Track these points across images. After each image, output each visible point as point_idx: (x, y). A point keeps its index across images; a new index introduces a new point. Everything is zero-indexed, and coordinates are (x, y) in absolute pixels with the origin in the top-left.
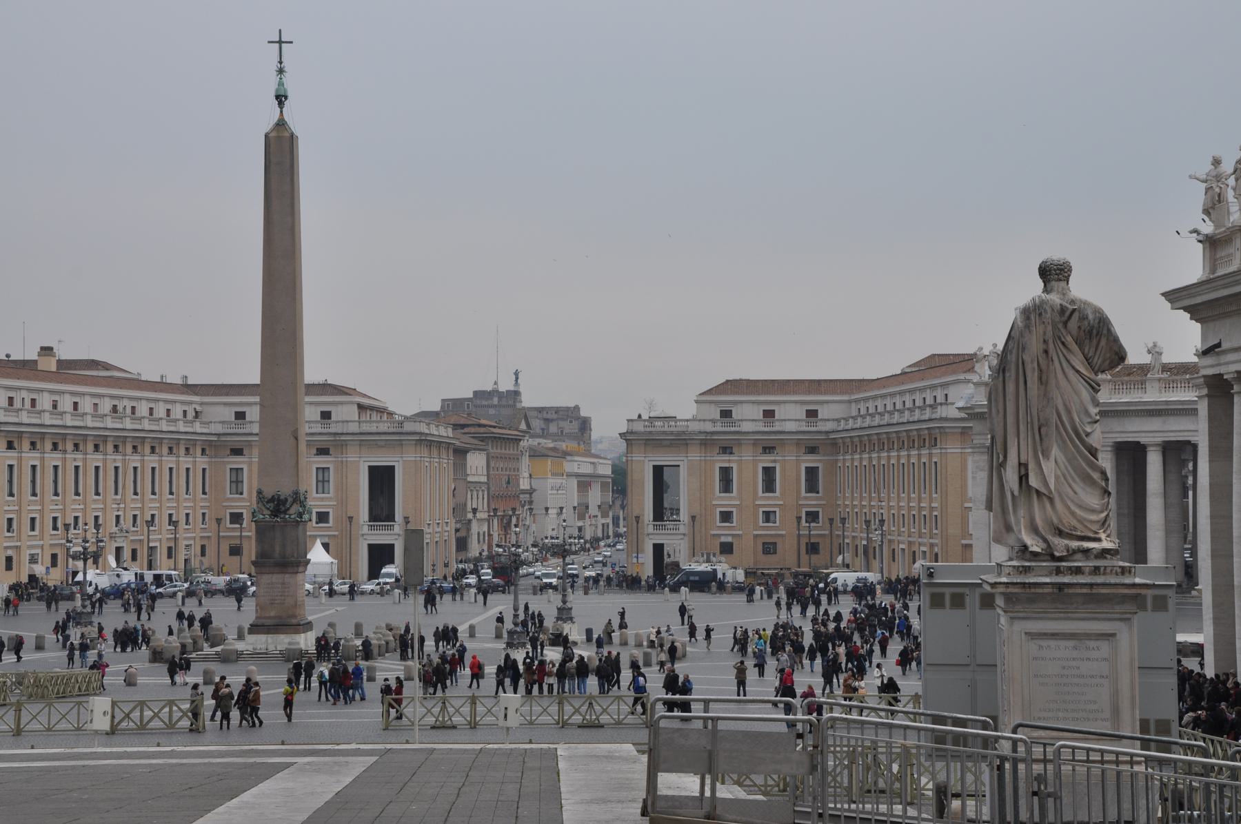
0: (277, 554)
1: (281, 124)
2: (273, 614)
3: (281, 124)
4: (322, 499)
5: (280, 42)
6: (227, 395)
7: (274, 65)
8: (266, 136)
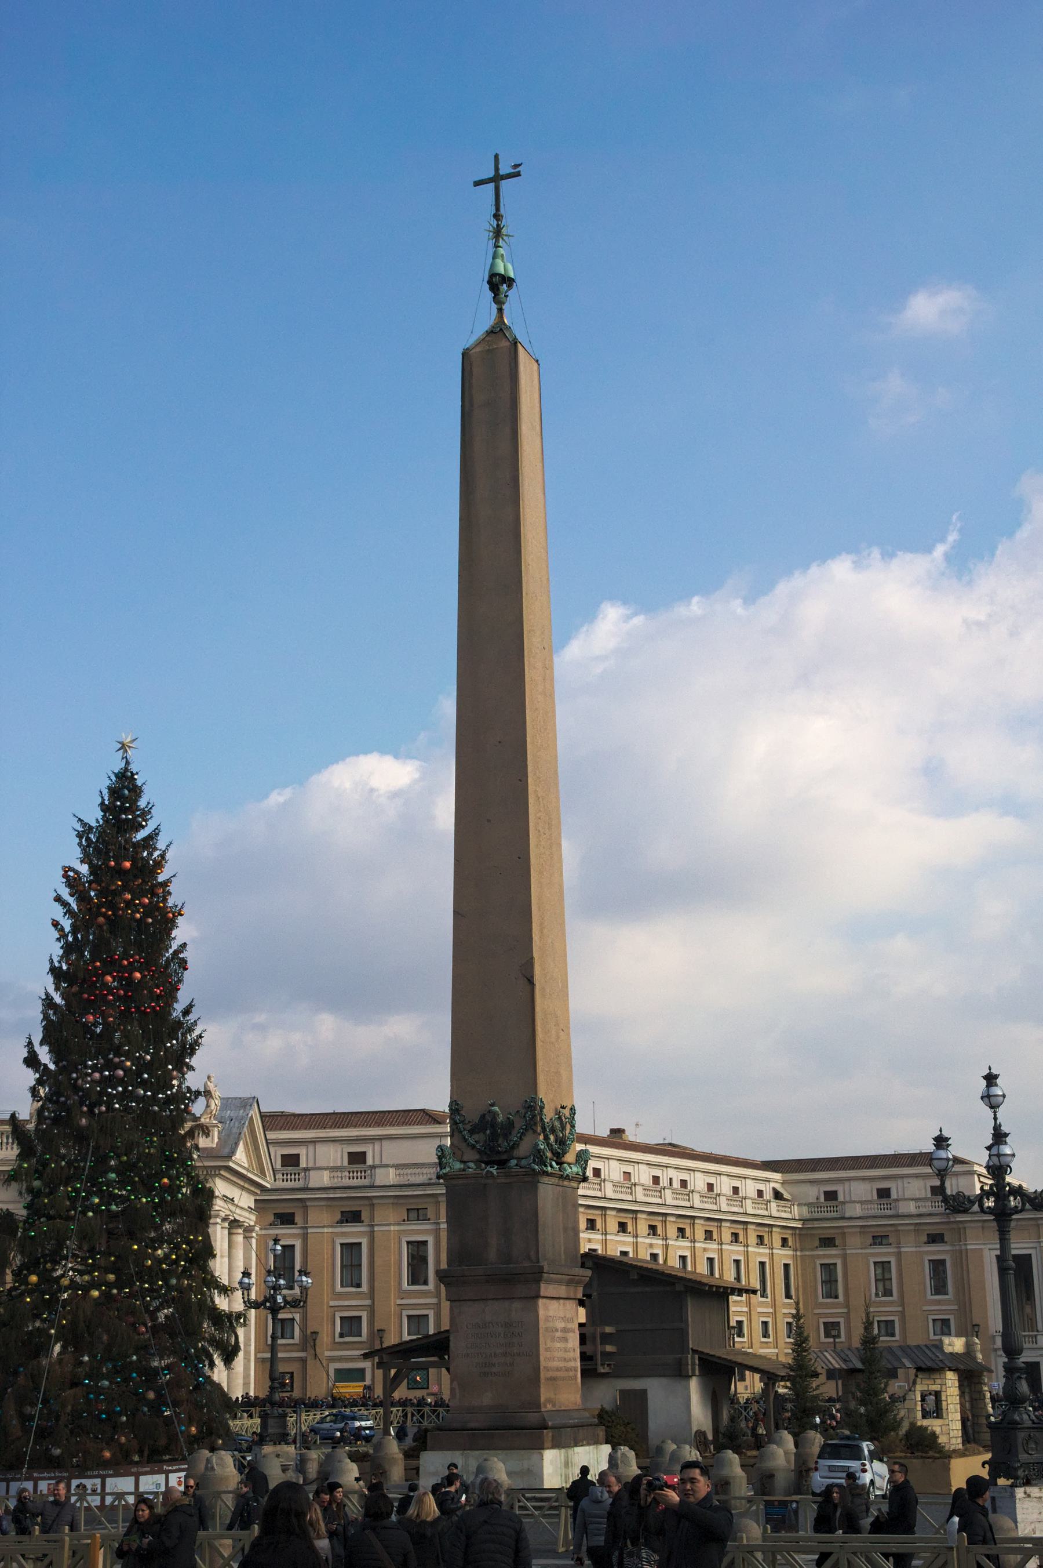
0: (492, 1254)
1: (498, 330)
2: (487, 1399)
3: (498, 330)
4: (939, 1302)
5: (497, 179)
6: (813, 1170)
7: (487, 221)
8: (465, 354)
